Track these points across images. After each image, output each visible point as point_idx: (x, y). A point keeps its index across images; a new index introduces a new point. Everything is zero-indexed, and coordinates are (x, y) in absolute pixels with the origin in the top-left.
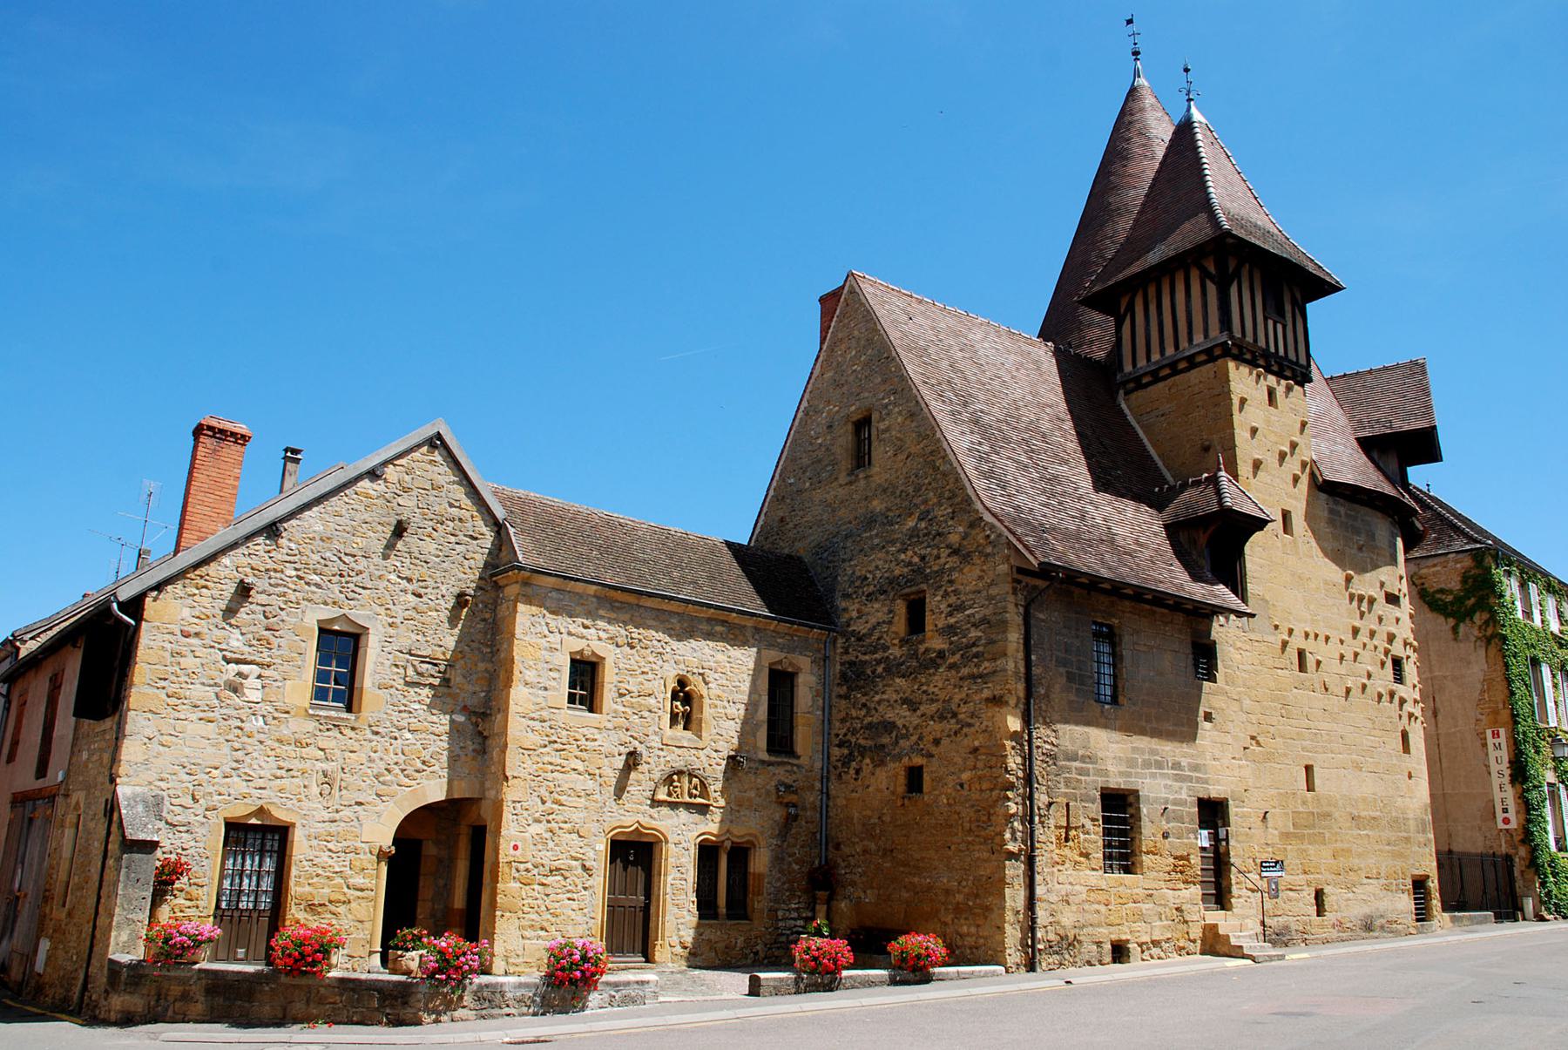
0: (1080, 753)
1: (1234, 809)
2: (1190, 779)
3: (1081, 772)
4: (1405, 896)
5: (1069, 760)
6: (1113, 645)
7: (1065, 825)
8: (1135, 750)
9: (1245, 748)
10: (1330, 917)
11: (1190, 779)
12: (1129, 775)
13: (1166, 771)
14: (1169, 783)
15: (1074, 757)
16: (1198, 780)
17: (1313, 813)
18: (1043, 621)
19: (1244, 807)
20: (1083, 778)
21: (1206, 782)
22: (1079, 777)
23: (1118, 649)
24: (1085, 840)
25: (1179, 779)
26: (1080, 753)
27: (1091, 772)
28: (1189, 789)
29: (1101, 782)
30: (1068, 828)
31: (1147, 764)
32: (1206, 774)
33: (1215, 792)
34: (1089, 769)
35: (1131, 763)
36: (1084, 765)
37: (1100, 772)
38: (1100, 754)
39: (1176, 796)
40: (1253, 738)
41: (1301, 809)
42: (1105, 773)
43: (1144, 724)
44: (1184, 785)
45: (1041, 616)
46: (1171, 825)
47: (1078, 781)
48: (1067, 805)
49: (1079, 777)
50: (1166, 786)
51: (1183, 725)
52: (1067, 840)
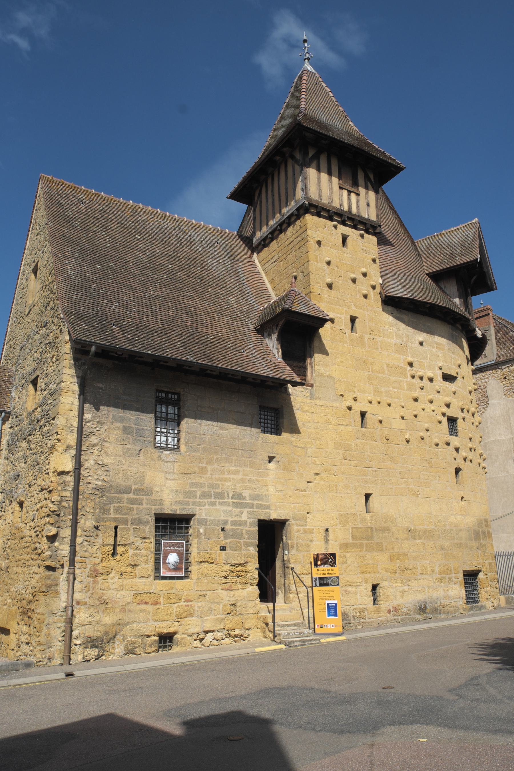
0: (133, 487)
1: (296, 528)
2: (251, 506)
3: (132, 502)
4: (457, 586)
5: (119, 492)
6: (179, 409)
7: (113, 543)
8: (193, 484)
9: (308, 482)
10: (384, 605)
11: (251, 506)
12: (188, 503)
13: (226, 500)
14: (229, 508)
15: (127, 490)
16: (259, 506)
17: (372, 528)
18: (101, 388)
19: (306, 525)
20: (135, 506)
21: (268, 507)
22: (131, 506)
23: (182, 410)
24: (133, 555)
25: (236, 505)
26: (133, 487)
27: (145, 502)
28: (249, 513)
29: (155, 509)
30: (115, 546)
31: (205, 495)
32: (268, 501)
33: (274, 515)
34: (142, 500)
35: (189, 494)
36: (137, 497)
37: (154, 502)
38: (156, 489)
39: (236, 518)
40: (317, 474)
41: (360, 526)
42: (161, 502)
43: (204, 465)
44: (245, 511)
45: (100, 385)
46: (228, 541)
47: (130, 509)
48: (116, 528)
49: (131, 506)
50: (225, 512)
51: (246, 466)
52: (114, 554)
